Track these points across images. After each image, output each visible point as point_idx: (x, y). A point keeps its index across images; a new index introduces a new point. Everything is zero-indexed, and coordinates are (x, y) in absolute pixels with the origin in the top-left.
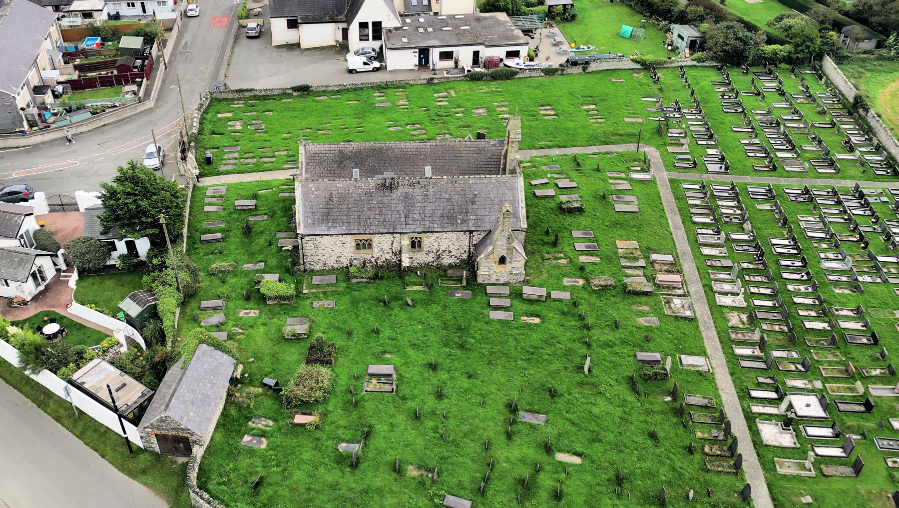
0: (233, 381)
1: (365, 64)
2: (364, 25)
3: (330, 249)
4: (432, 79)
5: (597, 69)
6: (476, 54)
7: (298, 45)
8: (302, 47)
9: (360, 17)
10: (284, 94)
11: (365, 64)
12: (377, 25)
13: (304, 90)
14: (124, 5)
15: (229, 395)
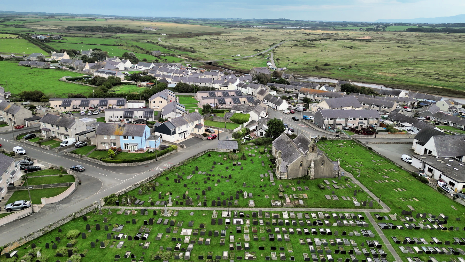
0: (234, 151)
1: (406, 158)
2: (426, 150)
3: (274, 150)
4: (401, 167)
5: (459, 202)
6: (441, 176)
7: (414, 150)
8: (415, 152)
9: (426, 146)
10: (366, 148)
11: (406, 158)
12: (430, 152)
13: (370, 149)
14: (416, 129)
15: (231, 151)
